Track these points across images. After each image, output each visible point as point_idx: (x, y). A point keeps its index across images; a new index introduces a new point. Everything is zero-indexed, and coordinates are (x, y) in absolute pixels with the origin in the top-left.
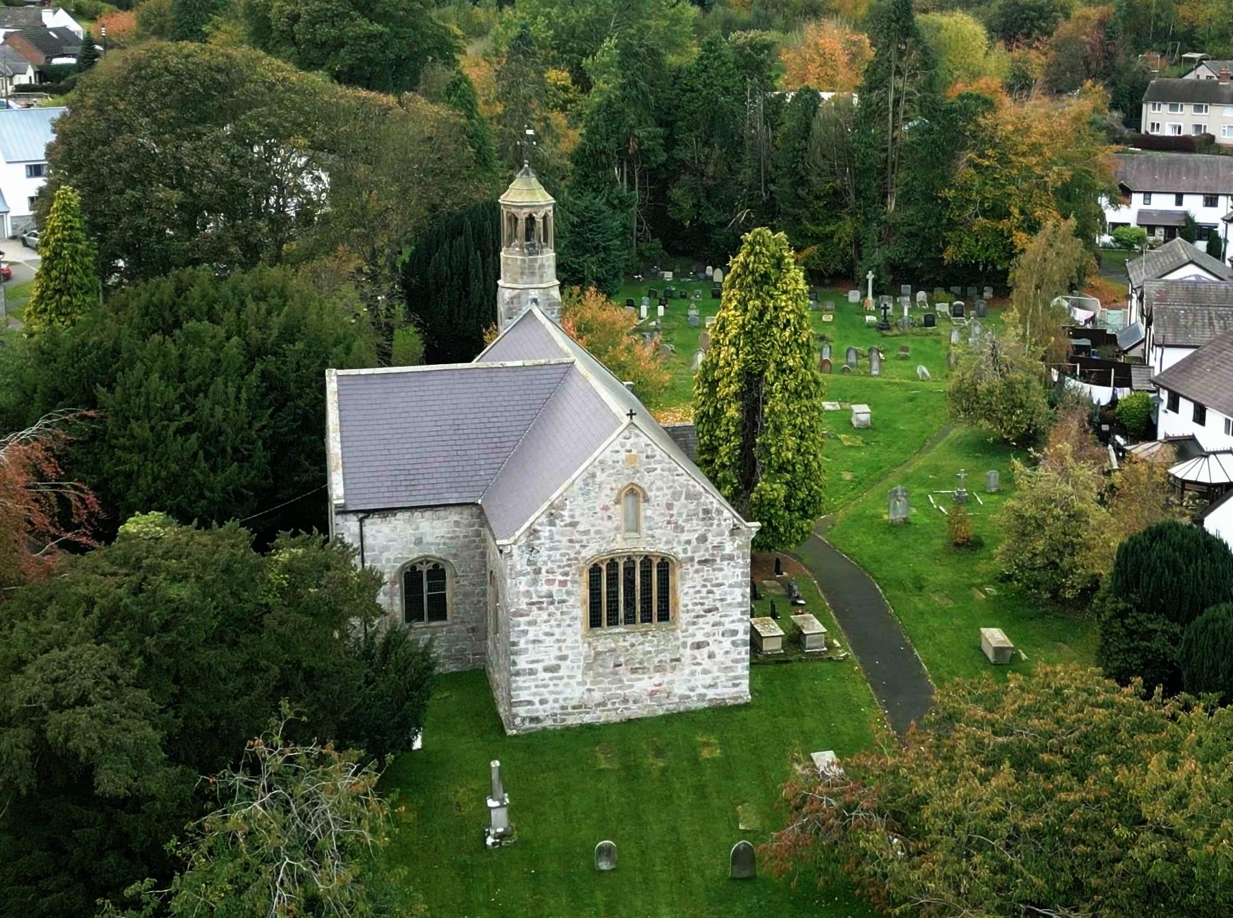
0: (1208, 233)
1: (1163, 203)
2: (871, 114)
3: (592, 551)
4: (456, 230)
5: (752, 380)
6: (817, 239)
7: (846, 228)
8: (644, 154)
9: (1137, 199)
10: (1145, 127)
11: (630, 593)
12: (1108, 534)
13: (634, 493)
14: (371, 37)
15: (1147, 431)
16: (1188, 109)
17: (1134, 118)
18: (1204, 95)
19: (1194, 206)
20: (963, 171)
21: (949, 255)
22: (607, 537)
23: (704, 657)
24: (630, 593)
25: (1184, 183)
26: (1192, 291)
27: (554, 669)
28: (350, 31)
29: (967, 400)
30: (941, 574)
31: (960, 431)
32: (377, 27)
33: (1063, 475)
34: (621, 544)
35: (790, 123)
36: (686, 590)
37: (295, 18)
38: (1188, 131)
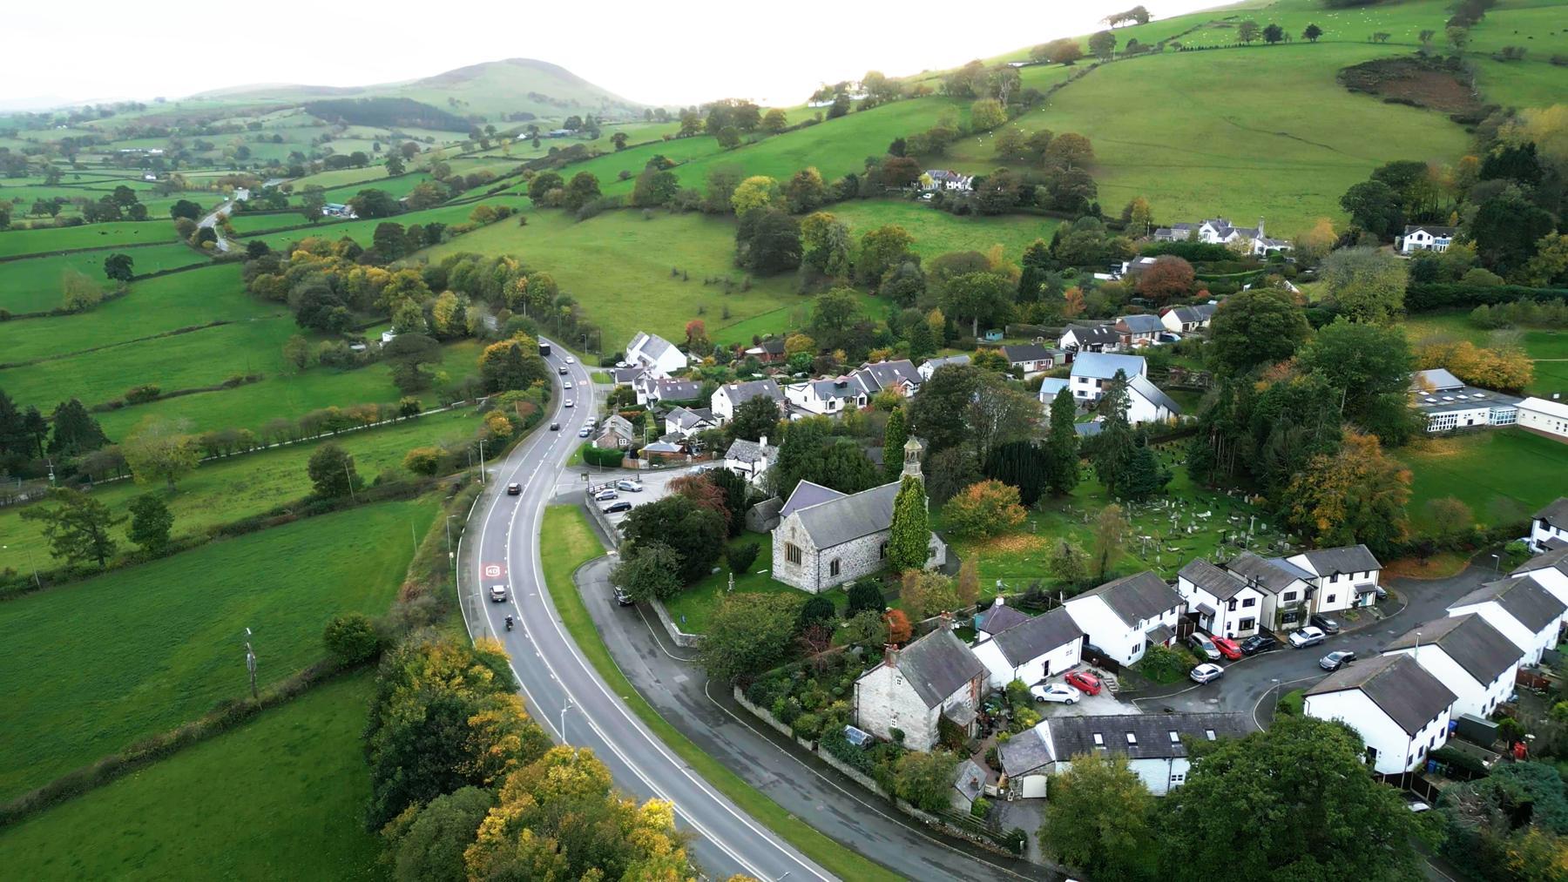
9: (1553, 530)
11: (794, 555)
13: (793, 529)
14: (1238, 343)
27: (780, 567)
28: (1232, 339)
32: (1243, 339)
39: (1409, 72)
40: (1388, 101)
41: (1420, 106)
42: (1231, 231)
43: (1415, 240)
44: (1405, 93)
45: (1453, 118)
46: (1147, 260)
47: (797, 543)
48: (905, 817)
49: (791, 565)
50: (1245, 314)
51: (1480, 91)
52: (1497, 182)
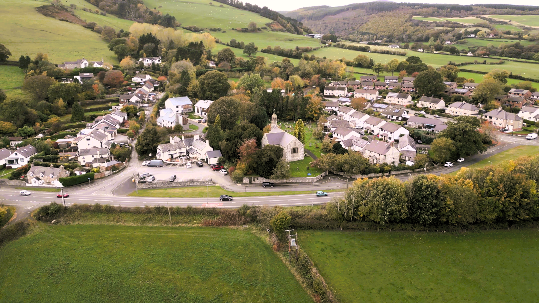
0: (335, 112)
1: (330, 108)
2: (296, 99)
3: (292, 147)
4: (257, 118)
5: (299, 133)
6: (289, 115)
7: (293, 113)
8: (266, 104)
10: (325, 94)
11: (295, 151)
12: (331, 146)
13: (295, 143)
15: (332, 137)
16: (331, 91)
17: (323, 92)
18: (333, 89)
19: (334, 108)
20: (308, 107)
21: (306, 117)
22: (293, 146)
23: (300, 156)
24: (295, 151)
25: (332, 105)
26: (335, 122)
29: (315, 134)
30: (316, 150)
31: (313, 137)
33: (326, 140)
34: (294, 147)
35: (285, 100)
36: (299, 150)
37: (209, 84)
38: (331, 94)
39: (57, 11)
40: (60, 20)
41: (71, 22)
42: (94, 63)
43: (147, 62)
44: (62, 18)
45: (83, 26)
46: (85, 74)
47: (297, 146)
48: (418, 172)
49: (294, 154)
50: (218, 78)
51: (82, 18)
52: (150, 44)
